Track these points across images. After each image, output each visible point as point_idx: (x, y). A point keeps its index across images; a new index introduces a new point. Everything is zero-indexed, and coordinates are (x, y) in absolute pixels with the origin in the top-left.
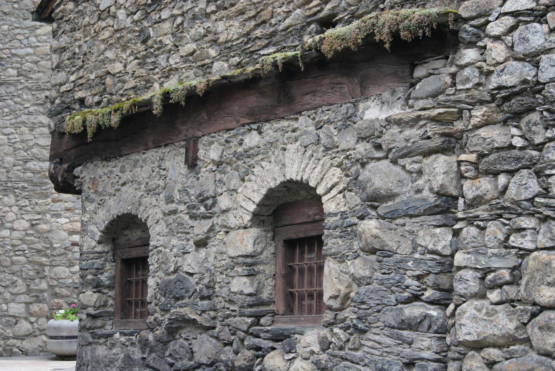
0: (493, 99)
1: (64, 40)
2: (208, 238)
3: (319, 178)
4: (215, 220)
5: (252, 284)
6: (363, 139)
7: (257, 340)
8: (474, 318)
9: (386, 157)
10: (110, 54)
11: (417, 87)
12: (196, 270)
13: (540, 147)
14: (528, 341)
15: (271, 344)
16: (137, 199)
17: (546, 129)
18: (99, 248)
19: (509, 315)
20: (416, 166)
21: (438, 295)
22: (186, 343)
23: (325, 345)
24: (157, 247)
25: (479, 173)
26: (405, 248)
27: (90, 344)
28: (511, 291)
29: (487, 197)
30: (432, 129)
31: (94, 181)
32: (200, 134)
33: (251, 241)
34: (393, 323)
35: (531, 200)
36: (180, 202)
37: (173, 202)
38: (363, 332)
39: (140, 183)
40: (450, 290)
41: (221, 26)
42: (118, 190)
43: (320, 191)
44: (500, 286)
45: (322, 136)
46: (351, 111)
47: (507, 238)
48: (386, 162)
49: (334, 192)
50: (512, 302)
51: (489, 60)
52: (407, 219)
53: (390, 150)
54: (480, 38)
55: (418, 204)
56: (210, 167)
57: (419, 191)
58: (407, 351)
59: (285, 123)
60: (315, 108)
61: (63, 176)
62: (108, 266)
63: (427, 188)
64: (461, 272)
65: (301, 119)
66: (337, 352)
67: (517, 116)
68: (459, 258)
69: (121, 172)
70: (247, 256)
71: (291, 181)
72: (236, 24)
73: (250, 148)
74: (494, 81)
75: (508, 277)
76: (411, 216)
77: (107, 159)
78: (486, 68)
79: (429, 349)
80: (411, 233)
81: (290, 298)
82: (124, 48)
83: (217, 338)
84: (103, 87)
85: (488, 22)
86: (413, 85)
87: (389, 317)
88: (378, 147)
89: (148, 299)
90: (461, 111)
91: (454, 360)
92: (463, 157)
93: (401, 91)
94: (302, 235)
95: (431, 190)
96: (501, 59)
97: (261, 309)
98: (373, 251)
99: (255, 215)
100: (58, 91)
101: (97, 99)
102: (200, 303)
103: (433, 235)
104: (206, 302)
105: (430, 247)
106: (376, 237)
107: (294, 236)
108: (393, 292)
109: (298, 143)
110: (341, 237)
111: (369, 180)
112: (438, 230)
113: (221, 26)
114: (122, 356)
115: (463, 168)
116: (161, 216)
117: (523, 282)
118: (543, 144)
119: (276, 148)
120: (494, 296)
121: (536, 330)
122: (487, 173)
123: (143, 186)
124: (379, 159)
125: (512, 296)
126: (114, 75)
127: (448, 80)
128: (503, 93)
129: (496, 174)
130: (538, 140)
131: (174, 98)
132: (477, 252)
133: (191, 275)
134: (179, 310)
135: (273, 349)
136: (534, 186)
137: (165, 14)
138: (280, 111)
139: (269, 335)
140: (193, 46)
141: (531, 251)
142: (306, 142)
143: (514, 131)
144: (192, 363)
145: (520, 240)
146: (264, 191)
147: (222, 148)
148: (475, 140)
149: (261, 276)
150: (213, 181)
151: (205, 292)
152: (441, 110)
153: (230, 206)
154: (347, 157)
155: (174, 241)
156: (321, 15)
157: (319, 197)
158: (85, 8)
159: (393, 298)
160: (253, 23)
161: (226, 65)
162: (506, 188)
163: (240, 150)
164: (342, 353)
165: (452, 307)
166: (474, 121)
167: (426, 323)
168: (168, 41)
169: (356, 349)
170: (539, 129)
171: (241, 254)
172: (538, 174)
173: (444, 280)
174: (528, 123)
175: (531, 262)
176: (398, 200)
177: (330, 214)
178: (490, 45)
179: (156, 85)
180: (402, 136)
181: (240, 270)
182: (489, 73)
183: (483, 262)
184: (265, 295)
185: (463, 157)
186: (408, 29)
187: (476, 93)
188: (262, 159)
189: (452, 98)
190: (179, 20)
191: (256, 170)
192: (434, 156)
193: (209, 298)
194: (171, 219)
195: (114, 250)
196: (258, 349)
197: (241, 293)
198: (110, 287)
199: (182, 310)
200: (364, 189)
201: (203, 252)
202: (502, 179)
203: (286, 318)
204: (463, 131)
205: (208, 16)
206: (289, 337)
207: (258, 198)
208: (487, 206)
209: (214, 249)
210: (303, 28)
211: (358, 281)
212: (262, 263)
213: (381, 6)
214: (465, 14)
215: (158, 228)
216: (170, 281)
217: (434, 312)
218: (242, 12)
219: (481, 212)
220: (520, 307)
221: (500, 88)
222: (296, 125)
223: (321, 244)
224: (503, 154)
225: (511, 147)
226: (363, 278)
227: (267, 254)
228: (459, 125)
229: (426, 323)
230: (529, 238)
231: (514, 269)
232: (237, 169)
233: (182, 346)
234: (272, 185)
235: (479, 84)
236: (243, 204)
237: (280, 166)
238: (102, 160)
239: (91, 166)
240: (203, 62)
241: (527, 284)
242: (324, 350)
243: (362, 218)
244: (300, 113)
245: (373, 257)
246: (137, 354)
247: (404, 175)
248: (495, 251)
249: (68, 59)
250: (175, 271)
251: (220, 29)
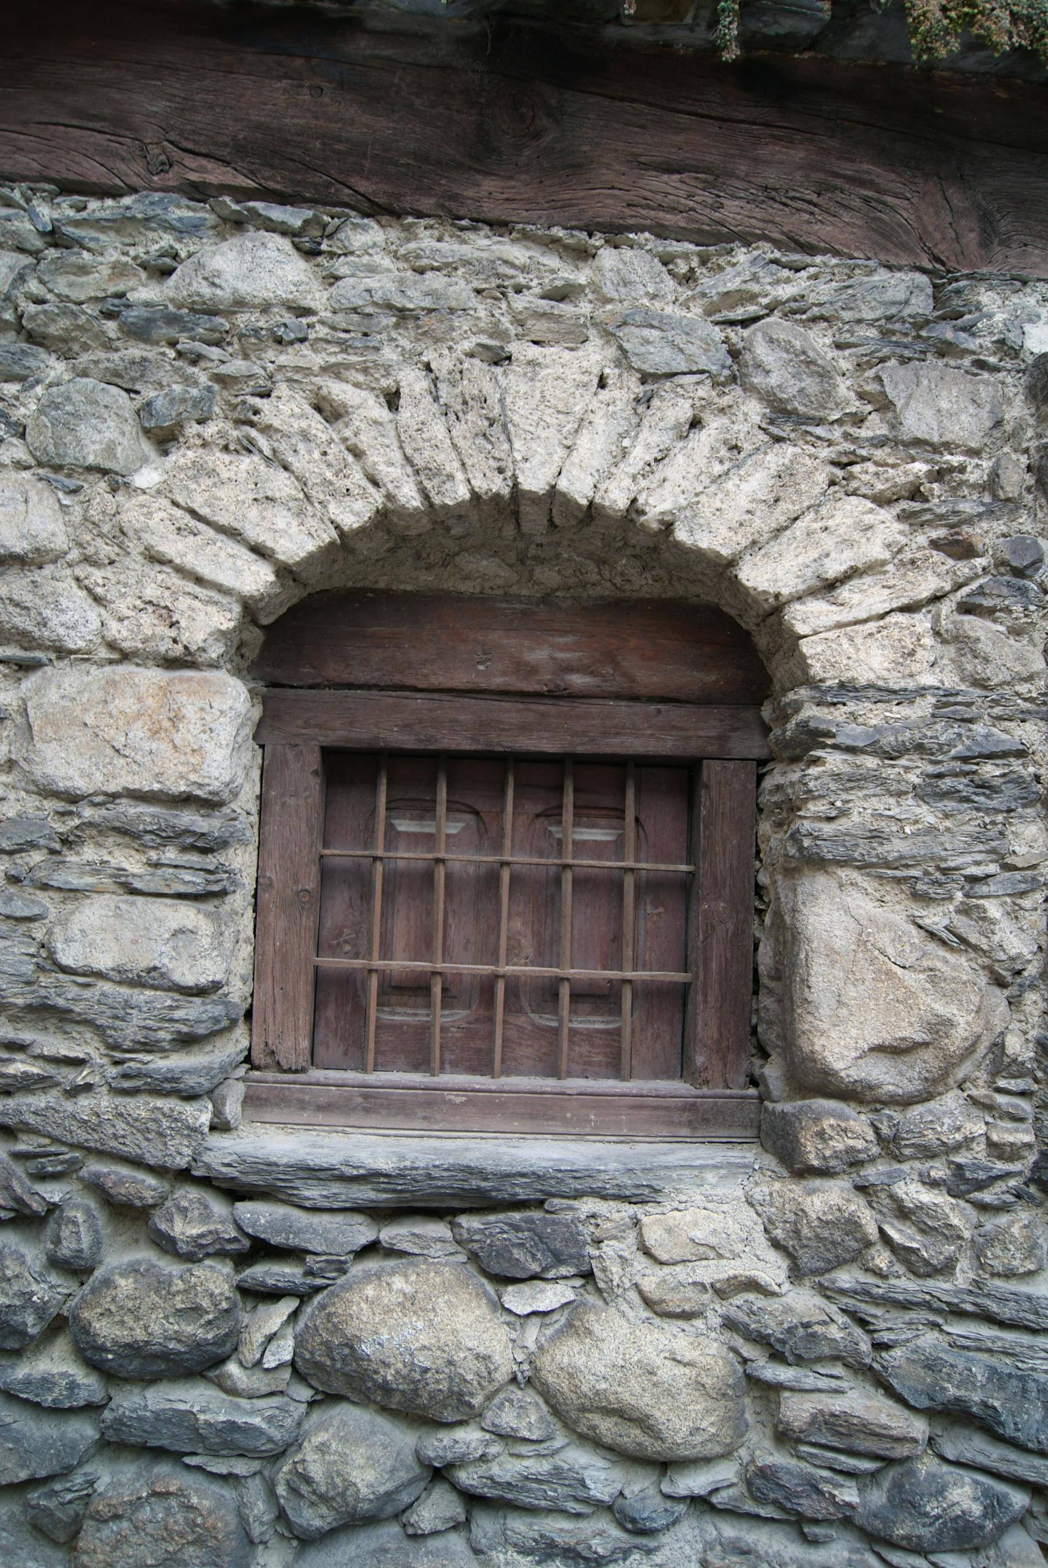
3: (763, 523)
15: (363, 1232)
45: (762, 351)
66: (906, 1285)
70: (186, 800)
73: (240, 304)
139: (365, 1194)
153: (60, 542)
164: (940, 1286)
181: (132, 863)
236: (172, 547)
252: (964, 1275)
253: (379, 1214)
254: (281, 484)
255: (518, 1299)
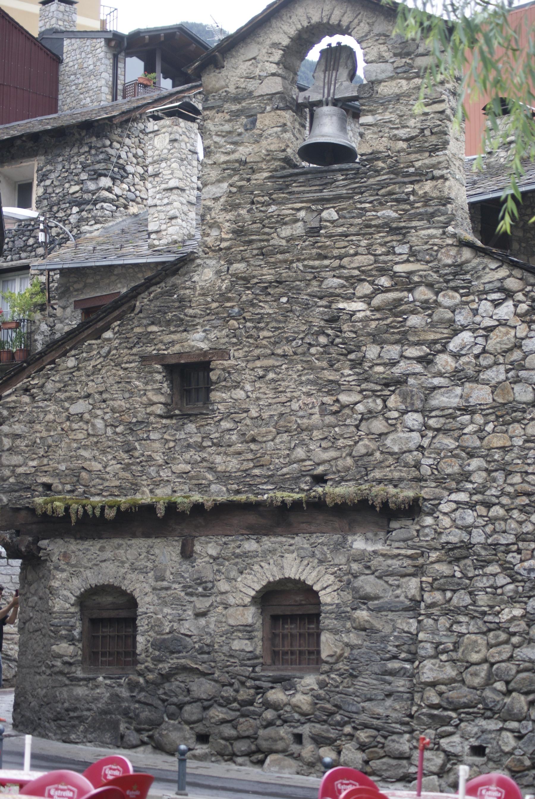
0: (443, 547)
1: (18, 428)
2: (209, 611)
3: (315, 580)
4: (213, 598)
5: (251, 645)
6: (355, 561)
7: (257, 683)
8: (431, 670)
9: (373, 574)
10: (86, 454)
11: (394, 533)
12: (195, 632)
13: (470, 579)
14: (463, 681)
15: (270, 685)
16: (120, 574)
17: (475, 569)
18: (73, 610)
19: (452, 667)
20: (397, 583)
21: (410, 656)
22: (183, 685)
23: (322, 685)
24: (146, 613)
25: (433, 589)
26: (387, 630)
27: (66, 685)
28: (454, 655)
29: (440, 603)
30: (407, 562)
31: (66, 556)
32: (197, 534)
33: (251, 616)
34: (378, 672)
35: (466, 607)
36: (174, 582)
37: (163, 580)
38: (356, 677)
39: (123, 562)
40: (415, 654)
41: (218, 459)
42: (97, 565)
43: (315, 588)
44: (447, 652)
45: (316, 552)
46: (340, 540)
47: (451, 626)
48: (372, 577)
49: (328, 590)
50: (453, 661)
51: (440, 525)
52: (390, 613)
53: (377, 570)
54: (435, 513)
55: (398, 605)
56: (207, 559)
57: (398, 597)
58: (388, 687)
59: (284, 539)
60: (312, 533)
61: (27, 547)
62: (78, 624)
63: (403, 595)
64: (422, 644)
65: (297, 538)
66: (333, 689)
67: (458, 560)
68: (421, 636)
69: (99, 550)
70: (246, 626)
71: (289, 578)
72: (235, 461)
74: (444, 539)
75: (452, 648)
76: (392, 611)
77: (83, 538)
78: (439, 530)
79: (403, 686)
80: (391, 620)
81: (275, 654)
82: (104, 452)
83: (216, 681)
84: (75, 479)
85: (440, 504)
86: (388, 532)
87: (376, 668)
88: (368, 568)
89: (138, 651)
90: (423, 553)
91: (418, 692)
92: (424, 579)
93: (382, 535)
94: (288, 613)
95: (406, 597)
96: (448, 526)
97: (256, 661)
98: (364, 630)
99: (253, 598)
100: (13, 471)
101: (68, 487)
102: (199, 656)
103: (408, 623)
104: (206, 656)
105: (406, 629)
106: (367, 621)
107: (280, 613)
108: (378, 654)
109: (295, 555)
110: (336, 619)
111: (362, 587)
112: (411, 620)
113: (218, 459)
114: (108, 695)
115: (424, 585)
116: (150, 590)
117: (461, 650)
118: (473, 577)
119: (275, 554)
120: (444, 657)
121: (468, 676)
122: (438, 589)
123: (127, 565)
124: (367, 574)
125: (455, 658)
126: (90, 471)
127: (415, 533)
128: (450, 546)
129: (444, 590)
130: (470, 575)
131: (180, 508)
132: (433, 633)
133: (190, 636)
134: (175, 661)
135: (272, 688)
136: (468, 600)
137: (153, 436)
138: (278, 530)
139: (269, 679)
140: (188, 467)
141: (465, 634)
142: (303, 554)
143: (456, 568)
144: (188, 699)
145: (459, 628)
146: (264, 583)
147: (219, 548)
148: (431, 570)
149: (256, 639)
150: (211, 571)
151: (206, 649)
152: (413, 552)
154: (340, 569)
155: (166, 610)
156: (316, 472)
157: (316, 593)
158: (48, 406)
159: (378, 658)
160: (251, 465)
161: (224, 489)
162: (451, 599)
163: (238, 551)
164: (337, 689)
165: (417, 663)
166: (431, 559)
167: (402, 672)
168: (159, 458)
169: (349, 687)
170: (472, 569)
171: (239, 623)
172: (470, 593)
173: (413, 648)
174: (465, 565)
175: (465, 640)
176: (381, 601)
177: (326, 604)
178: (441, 517)
179: (147, 490)
180: (385, 563)
181: (240, 635)
182: (441, 533)
183: (437, 639)
184: (258, 652)
185: (424, 579)
186: (395, 503)
187: (432, 543)
188: (261, 561)
189: (418, 544)
190: (172, 444)
191: (256, 567)
192: (408, 578)
193: (209, 653)
194: (163, 594)
195: (81, 610)
196: (258, 688)
197: (243, 651)
198: (79, 641)
199: (183, 661)
200: (357, 592)
201: (202, 621)
202: (449, 594)
203: (273, 667)
204: (423, 565)
205: (202, 448)
206: (289, 680)
207: (258, 587)
208: (439, 608)
209: (213, 619)
210: (298, 478)
211: (353, 647)
212: (257, 631)
213: (366, 478)
214: (426, 497)
215: (147, 599)
216: (164, 640)
217: (408, 666)
218: (240, 453)
219: (435, 611)
220: (458, 663)
221: (448, 543)
222: (292, 542)
223: (318, 622)
224: (449, 580)
225: (454, 576)
226: (356, 645)
227: (258, 624)
228: (421, 561)
229: (402, 672)
230: (464, 627)
231: (455, 643)
232: (236, 564)
233: (178, 687)
234: (271, 579)
235: (434, 538)
236: (243, 590)
237: (279, 567)
238: (76, 539)
239: (60, 542)
240: (200, 482)
241: (463, 651)
242: (321, 688)
243: (355, 609)
244: (297, 535)
245: (364, 633)
246: (125, 693)
247: (386, 586)
248: (445, 633)
249: (26, 446)
250: (170, 632)
251: (217, 461)
252: (341, 687)
253: (273, 682)
254: (255, 579)
255: (287, 693)
